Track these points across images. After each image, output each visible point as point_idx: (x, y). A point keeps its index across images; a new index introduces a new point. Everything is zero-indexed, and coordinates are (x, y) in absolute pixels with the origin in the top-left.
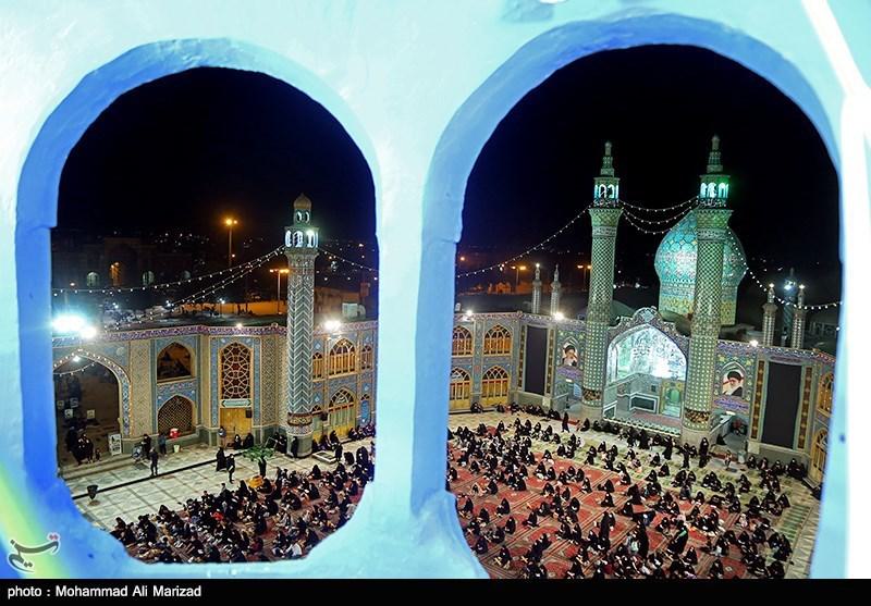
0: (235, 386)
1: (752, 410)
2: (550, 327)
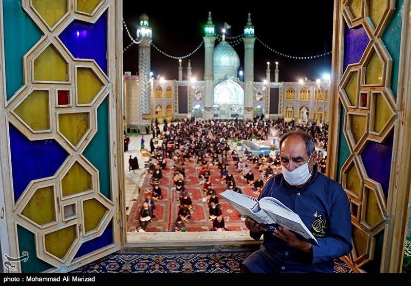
1: (263, 107)
2: (189, 86)
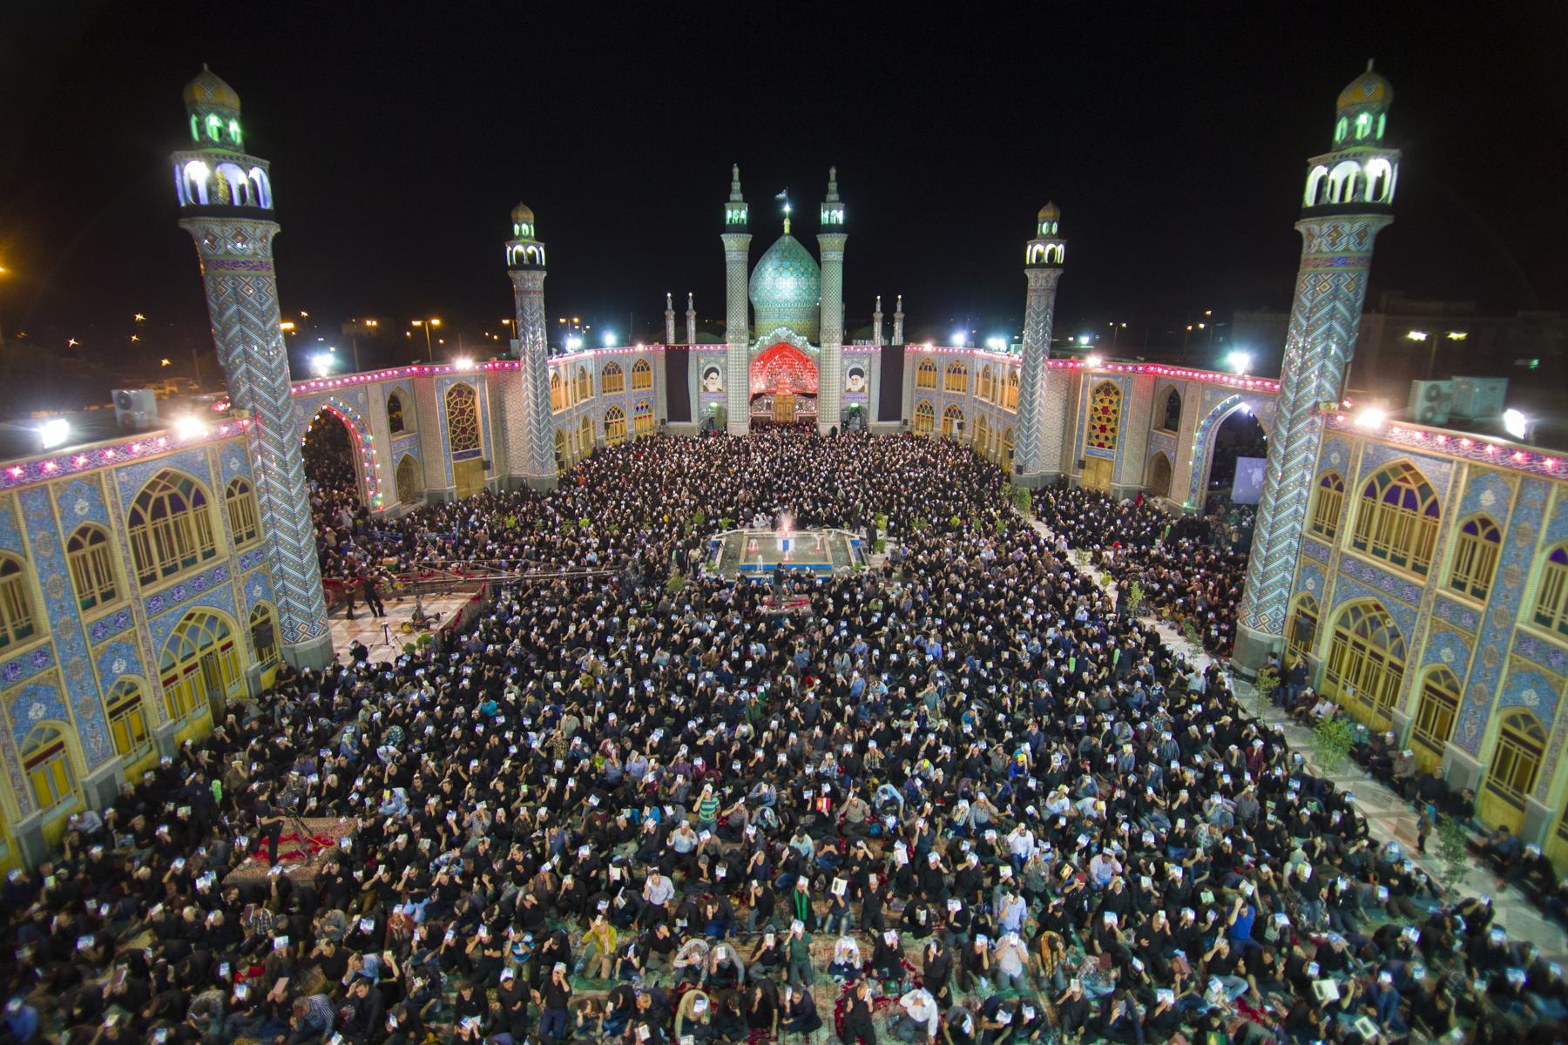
0: (464, 436)
